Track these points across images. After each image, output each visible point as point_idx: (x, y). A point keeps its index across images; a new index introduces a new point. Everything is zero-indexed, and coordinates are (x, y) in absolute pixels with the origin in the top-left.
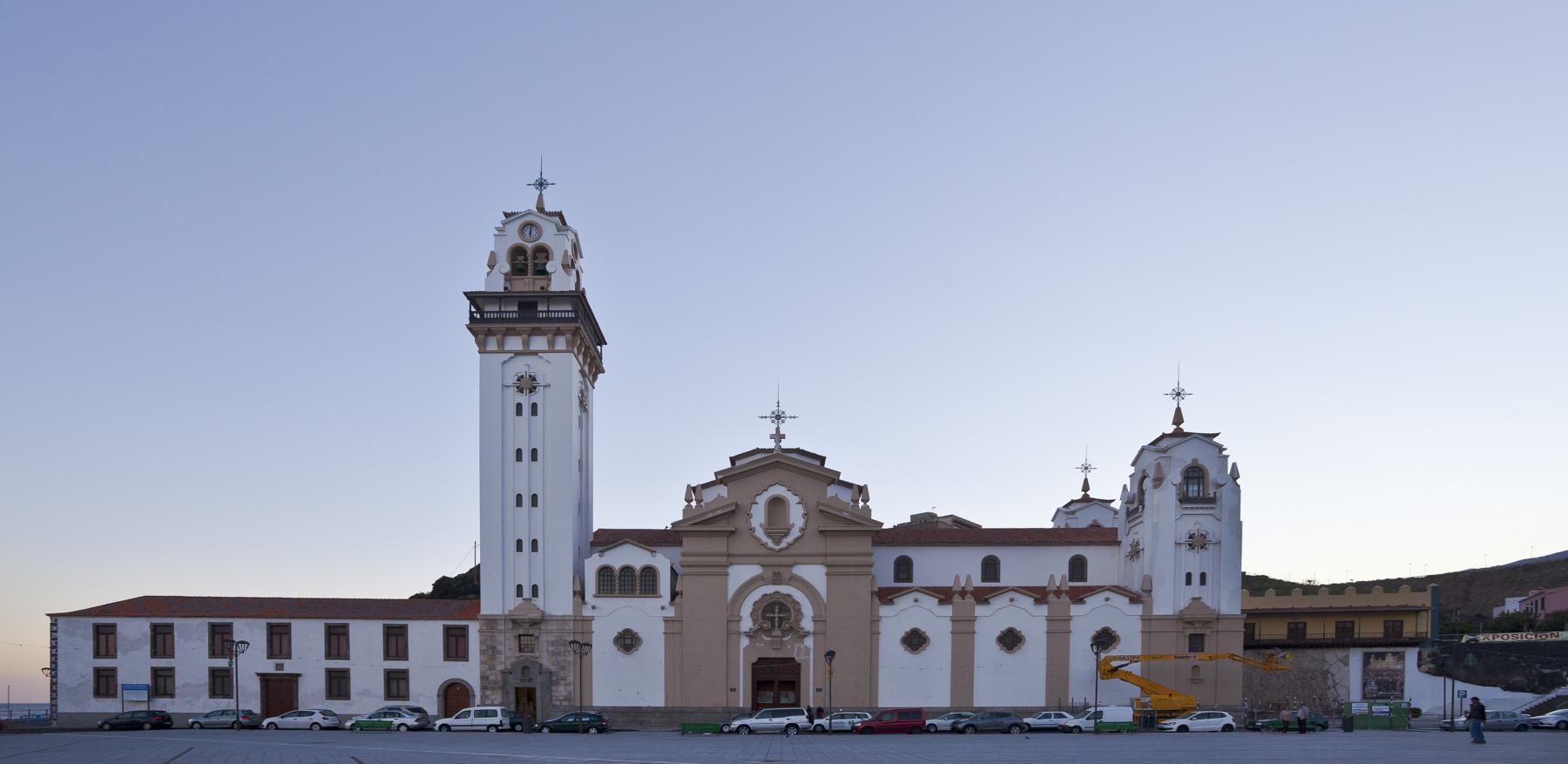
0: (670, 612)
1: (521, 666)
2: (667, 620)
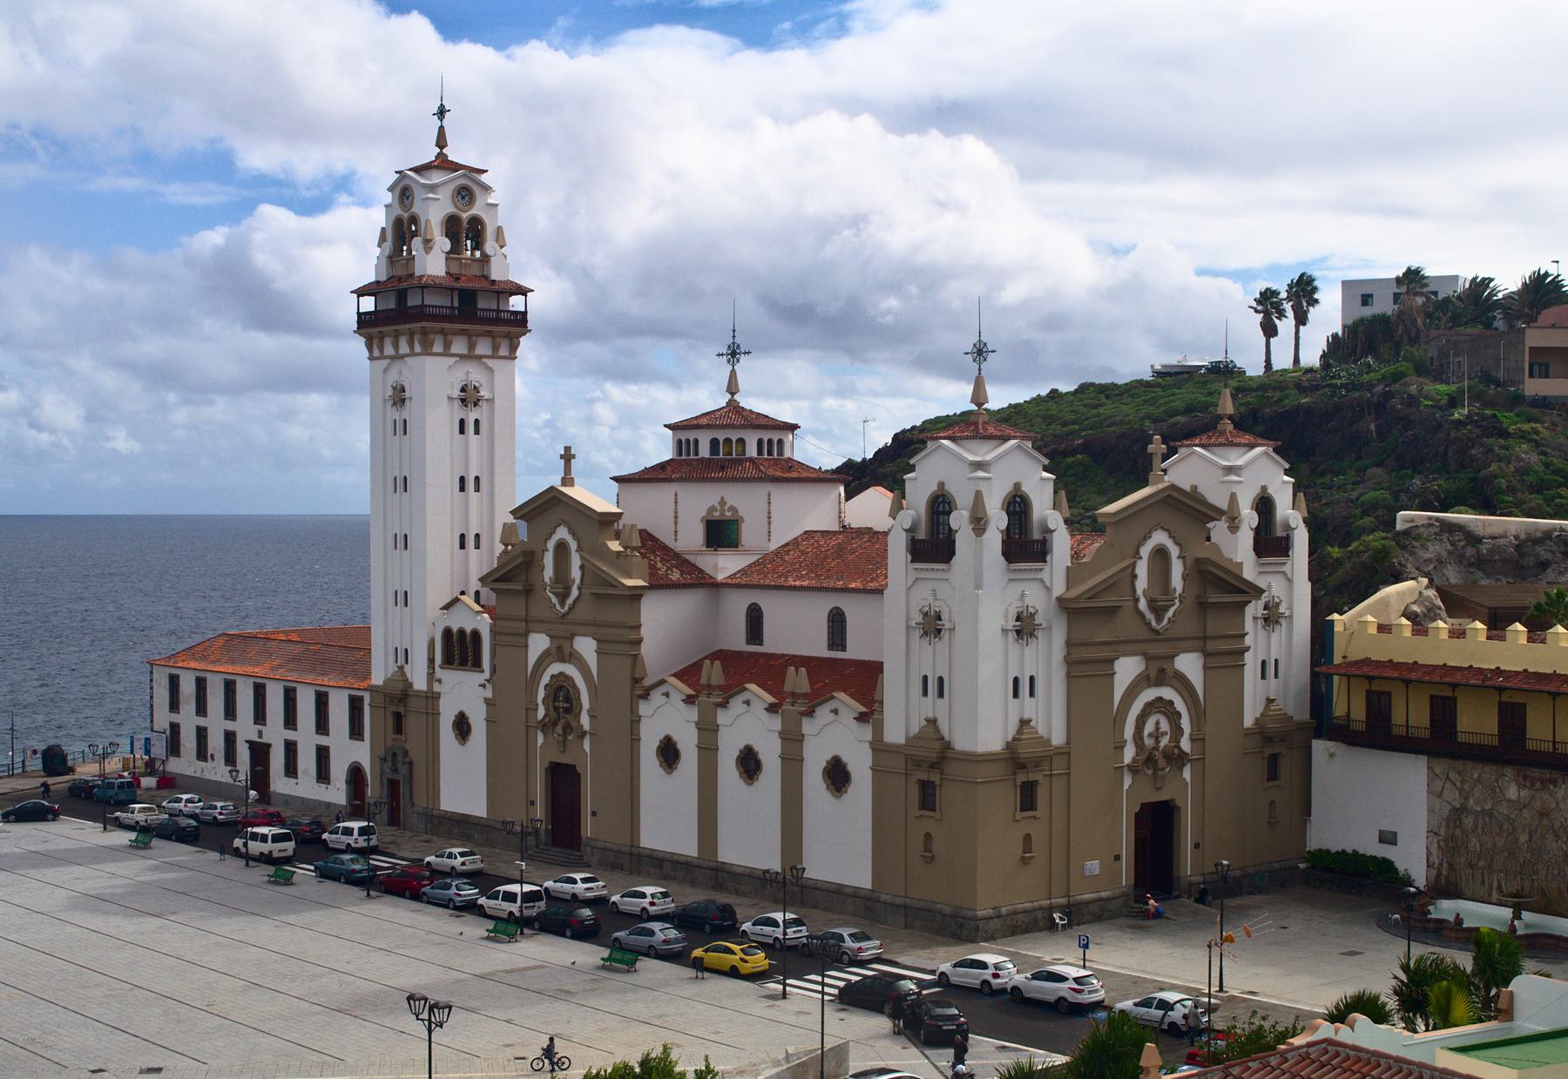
0: (489, 694)
1: (391, 752)
2: (486, 700)
